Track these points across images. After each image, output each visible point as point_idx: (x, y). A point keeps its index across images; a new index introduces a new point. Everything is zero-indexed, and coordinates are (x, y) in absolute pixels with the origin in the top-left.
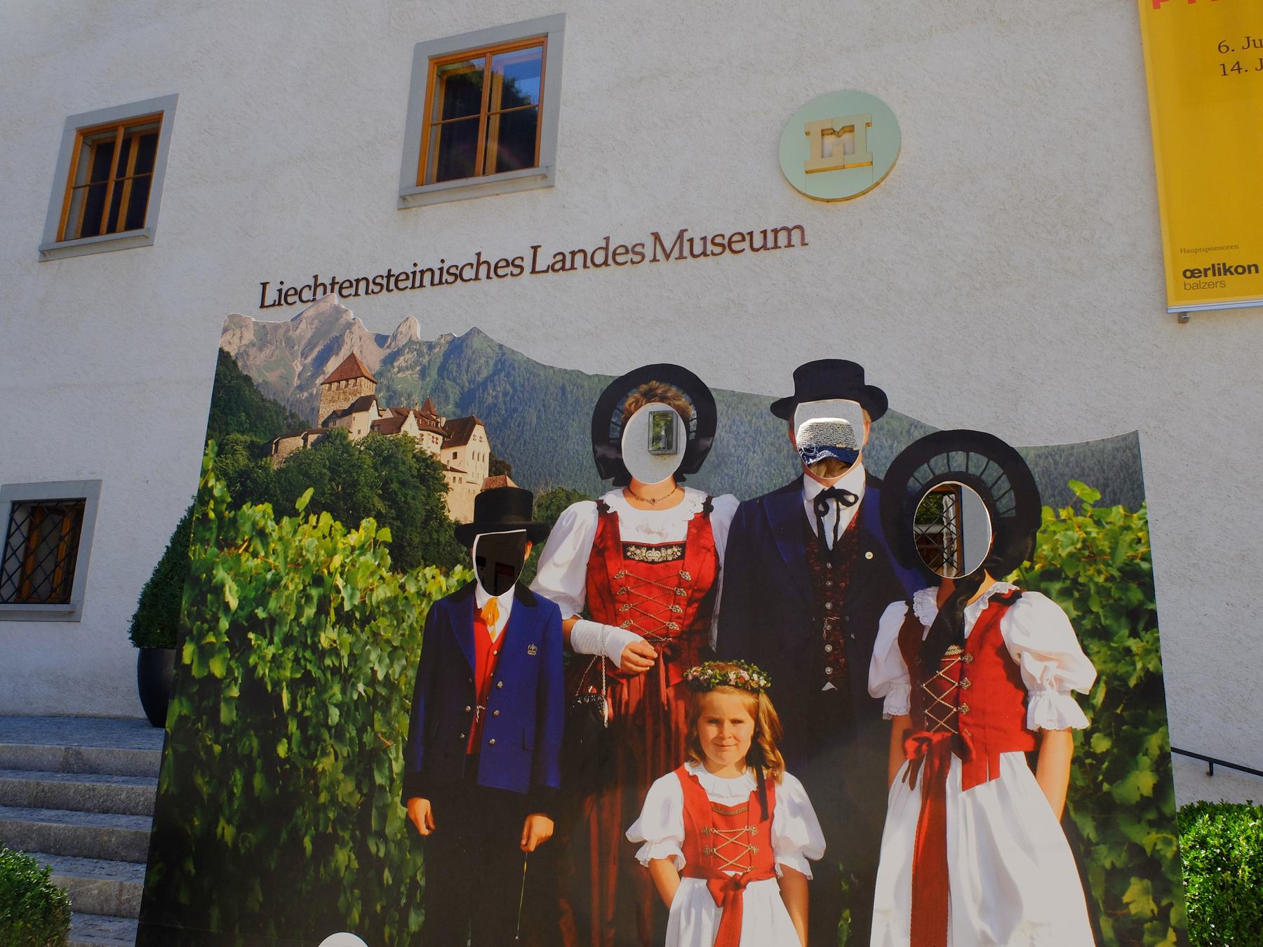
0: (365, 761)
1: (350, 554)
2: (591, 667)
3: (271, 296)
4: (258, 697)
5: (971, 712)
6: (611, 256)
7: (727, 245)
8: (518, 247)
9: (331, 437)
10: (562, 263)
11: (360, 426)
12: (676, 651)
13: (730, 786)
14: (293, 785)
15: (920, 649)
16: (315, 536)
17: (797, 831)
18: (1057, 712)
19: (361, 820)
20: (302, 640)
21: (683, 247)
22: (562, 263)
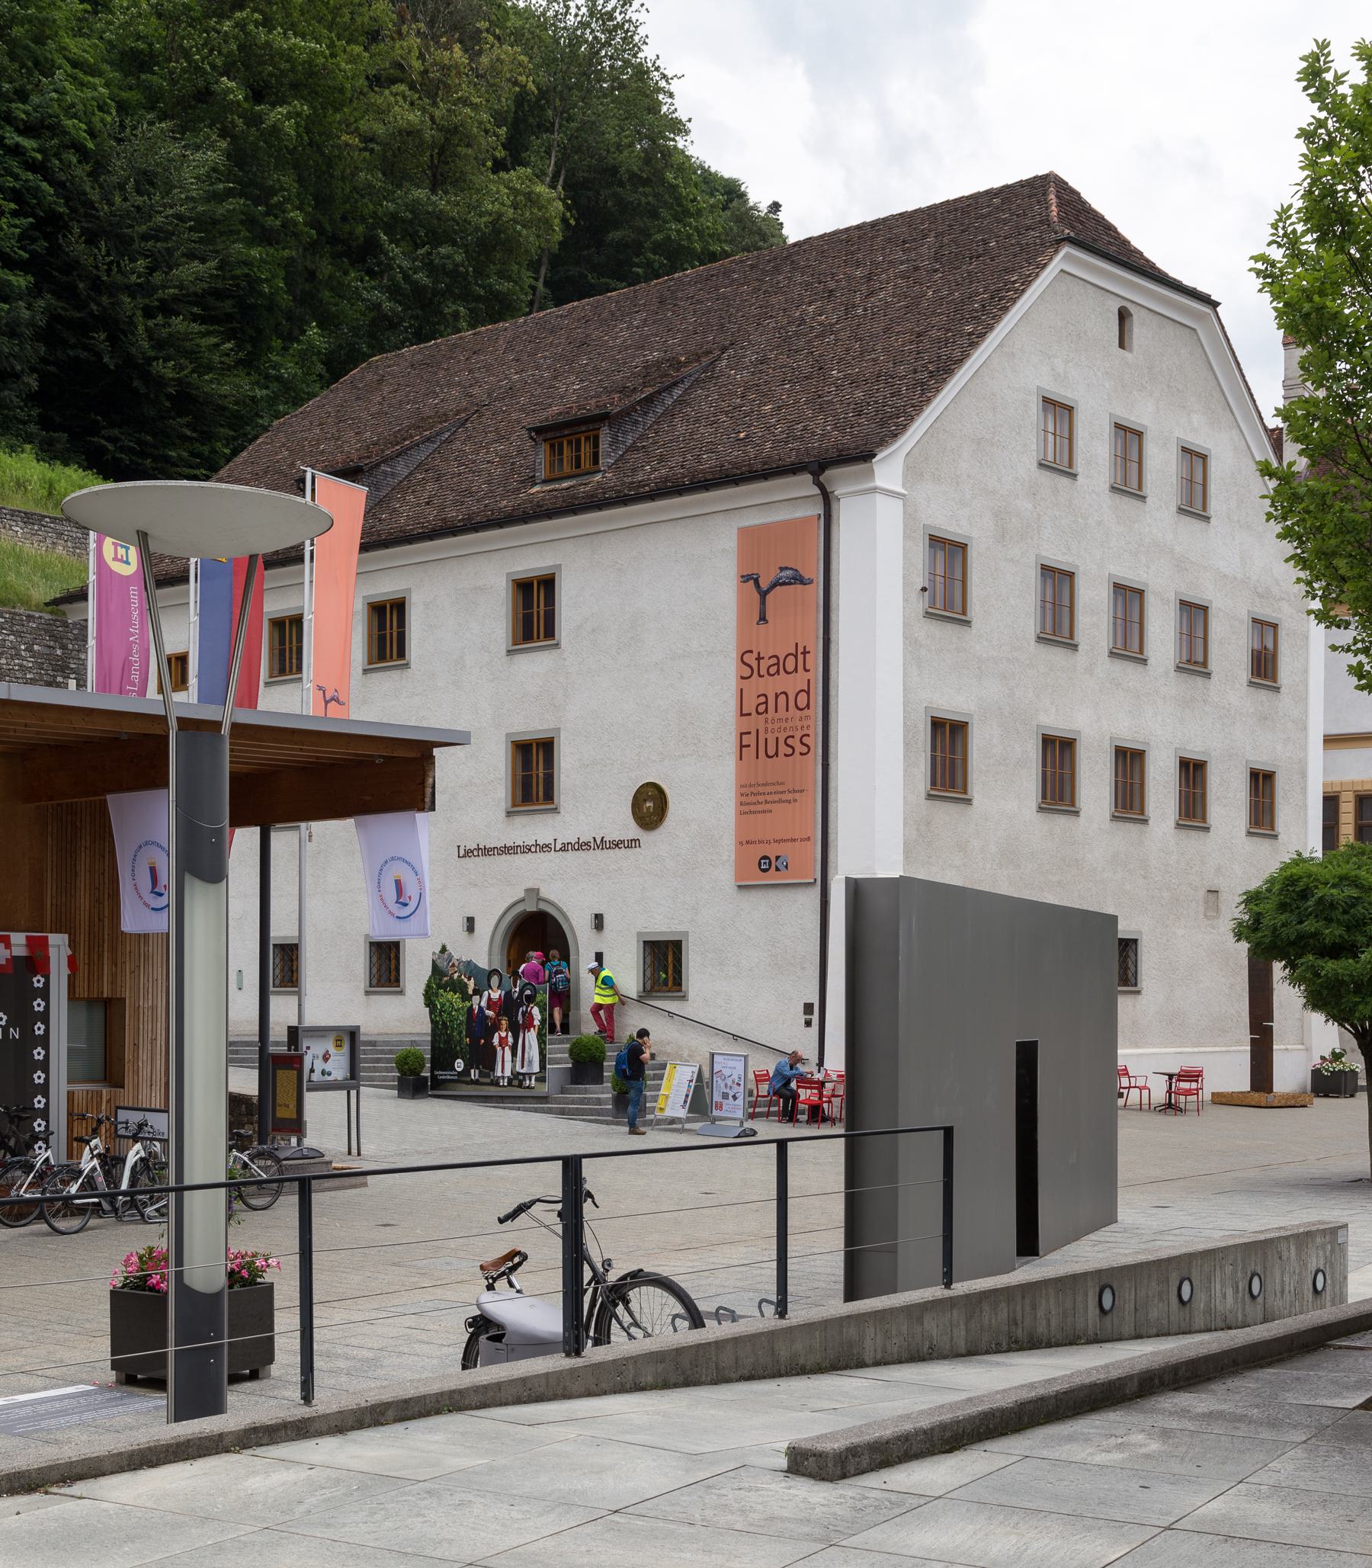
0: (460, 1033)
1: (455, 998)
2: (487, 1017)
3: (462, 853)
4: (444, 1024)
5: (529, 1024)
6: (581, 846)
7: (617, 844)
8: (549, 840)
9: (452, 978)
10: (564, 848)
11: (456, 976)
12: (498, 1015)
13: (503, 1034)
14: (450, 1037)
15: (524, 1014)
16: (450, 995)
17: (510, 1040)
18: (536, 1023)
19: (460, 1042)
20: (450, 1014)
21: (602, 844)
22: (564, 848)
